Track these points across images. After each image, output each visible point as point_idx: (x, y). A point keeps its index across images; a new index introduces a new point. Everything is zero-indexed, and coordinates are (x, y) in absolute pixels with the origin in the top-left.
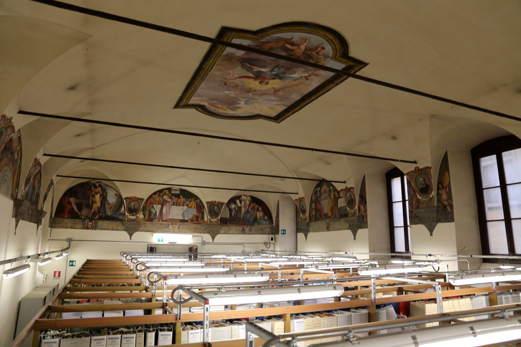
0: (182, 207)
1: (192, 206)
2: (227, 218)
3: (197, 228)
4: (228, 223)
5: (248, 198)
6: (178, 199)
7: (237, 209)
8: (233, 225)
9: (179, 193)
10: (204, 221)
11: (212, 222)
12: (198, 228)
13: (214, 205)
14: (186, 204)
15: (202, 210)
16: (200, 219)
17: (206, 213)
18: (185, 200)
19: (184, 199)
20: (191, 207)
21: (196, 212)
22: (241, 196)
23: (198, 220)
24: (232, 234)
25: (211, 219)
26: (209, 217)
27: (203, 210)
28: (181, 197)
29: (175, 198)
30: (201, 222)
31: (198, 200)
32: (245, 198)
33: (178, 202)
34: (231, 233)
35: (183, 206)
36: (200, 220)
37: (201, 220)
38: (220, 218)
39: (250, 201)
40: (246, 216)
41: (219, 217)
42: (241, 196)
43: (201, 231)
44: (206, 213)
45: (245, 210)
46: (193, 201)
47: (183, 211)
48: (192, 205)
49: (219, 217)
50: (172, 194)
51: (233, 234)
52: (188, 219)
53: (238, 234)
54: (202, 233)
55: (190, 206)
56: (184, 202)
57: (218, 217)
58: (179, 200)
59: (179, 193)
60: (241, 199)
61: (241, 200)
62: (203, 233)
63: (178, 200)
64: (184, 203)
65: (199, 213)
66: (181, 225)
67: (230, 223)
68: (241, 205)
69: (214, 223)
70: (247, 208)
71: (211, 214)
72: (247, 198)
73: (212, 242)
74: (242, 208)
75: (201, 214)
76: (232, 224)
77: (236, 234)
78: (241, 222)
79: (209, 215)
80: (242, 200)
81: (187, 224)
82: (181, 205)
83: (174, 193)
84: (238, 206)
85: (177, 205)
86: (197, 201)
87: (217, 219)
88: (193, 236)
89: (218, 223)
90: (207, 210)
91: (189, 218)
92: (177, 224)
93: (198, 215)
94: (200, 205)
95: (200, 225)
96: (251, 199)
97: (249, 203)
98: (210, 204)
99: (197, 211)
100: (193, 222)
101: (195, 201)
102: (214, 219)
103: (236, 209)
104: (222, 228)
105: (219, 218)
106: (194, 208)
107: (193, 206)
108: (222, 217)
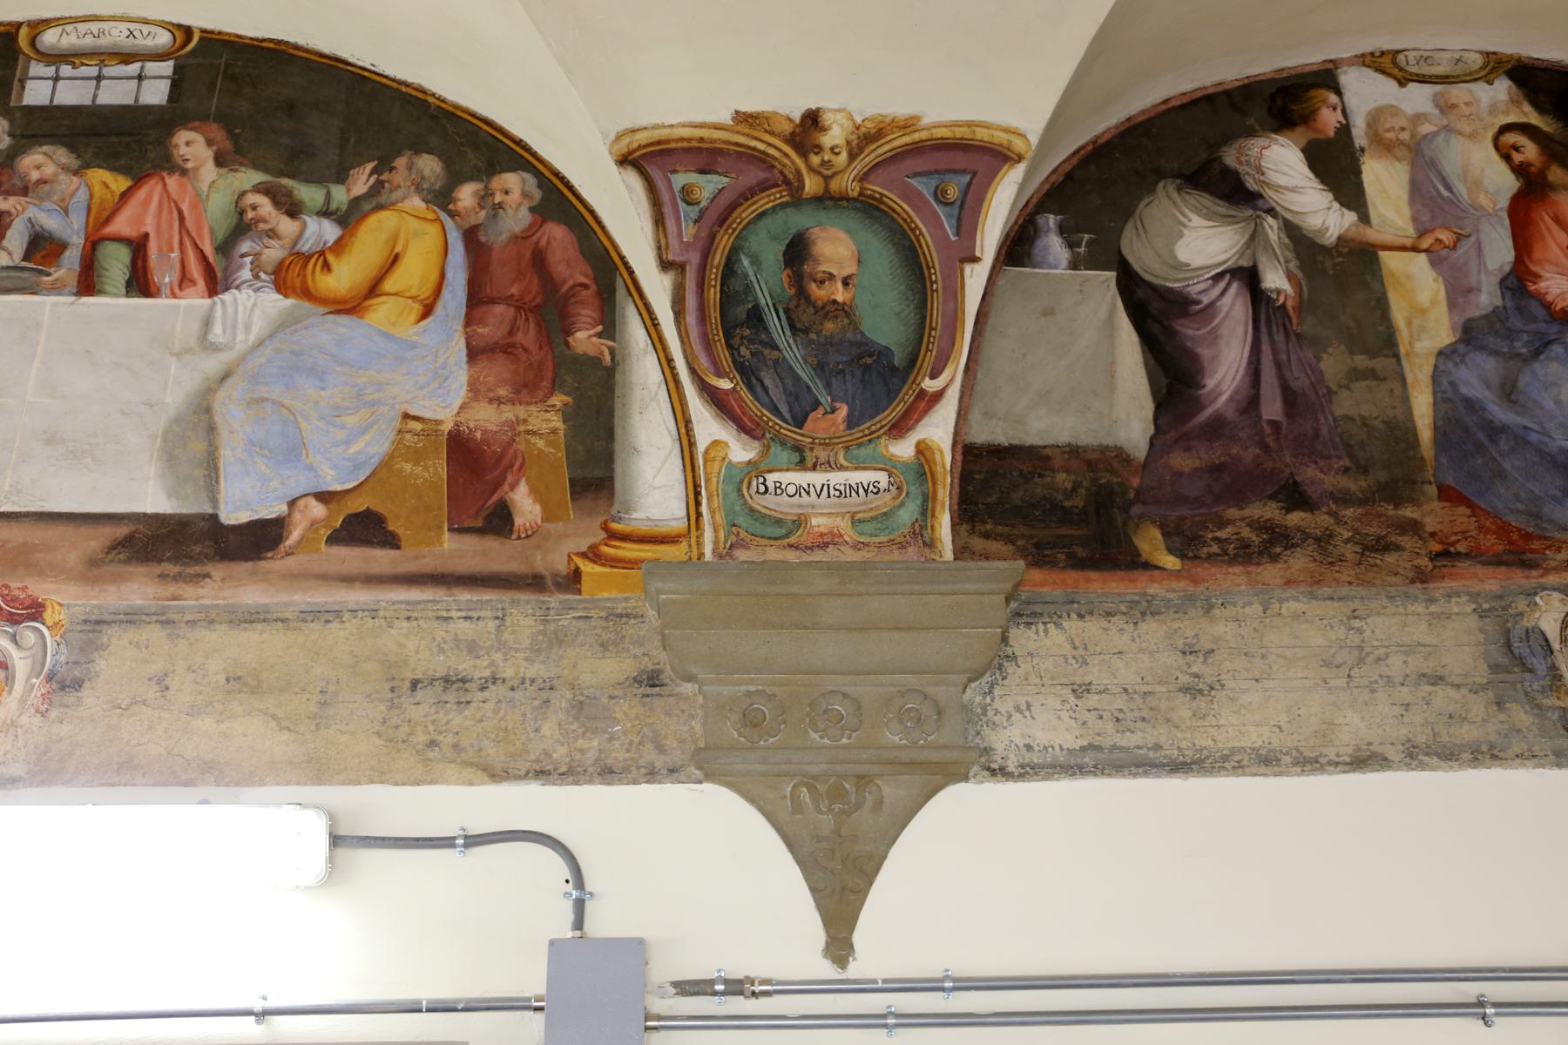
0: (195, 302)
1: (389, 285)
2: (1113, 457)
3: (464, 665)
4: (1150, 542)
5: (1458, 92)
6: (120, 183)
7: (1290, 276)
8: (1270, 572)
9: (156, 93)
10: (614, 536)
11: (787, 529)
12: (478, 668)
13: (797, 199)
14: (274, 253)
15: (584, 339)
16: (537, 493)
17: (667, 362)
18: (253, 198)
19: (251, 177)
20: (373, 289)
21: (460, 376)
22: (1326, 78)
23: (500, 521)
24: (1267, 761)
25: (755, 469)
26: (709, 427)
27: (609, 326)
28: (192, 145)
29: (76, 173)
30: (556, 560)
31: (513, 182)
32: (1417, 98)
33: (122, 225)
34: (1258, 737)
35: (216, 284)
36: (525, 505)
37: (548, 516)
38: (971, 455)
39: (1530, 151)
40: (1509, 392)
41: (938, 429)
42: (1326, 78)
43: (550, 735)
44: (667, 362)
45: (1458, 292)
46: (416, 203)
47: (212, 364)
48: (396, 259)
49: (938, 429)
50: (31, 110)
51: (1309, 763)
52: (272, 509)
53: (1415, 755)
54: (571, 774)
55: (343, 277)
56: (242, 227)
57: (899, 428)
58: (151, 191)
59: (156, 93)
60: (1329, 120)
61: (1345, 130)
62: (608, 773)
63: (125, 196)
64: (226, 247)
65: (527, 388)
66: (132, 618)
67: (1185, 542)
68: (1364, 218)
69: (827, 541)
70: (1499, 251)
71: (747, 373)
72: (1446, 108)
73: (827, 970)
74: (1391, 262)
75: (558, 400)
76: (1244, 555)
77: (1363, 760)
78: (1433, 514)
79: (718, 401)
80: (1359, 136)
81: (251, 595)
82: (165, 276)
83: (72, 94)
84: (1293, 231)
85: (88, 284)
86: (484, 197)
87: (890, 466)
88: (336, 840)
89: (921, 534)
90: (657, 287)
91: (300, 483)
92: (35, 611)
93: (487, 418)
94: (539, 260)
95: (523, 612)
96: (1533, 118)
97: (1520, 170)
98: (708, 186)
99: (474, 354)
100: (380, 559)
101: (442, 198)
102: (831, 466)
103: (1275, 279)
104: (1023, 639)
105: (922, 450)
106: (427, 311)
107: (413, 274)
108: (984, 433)
